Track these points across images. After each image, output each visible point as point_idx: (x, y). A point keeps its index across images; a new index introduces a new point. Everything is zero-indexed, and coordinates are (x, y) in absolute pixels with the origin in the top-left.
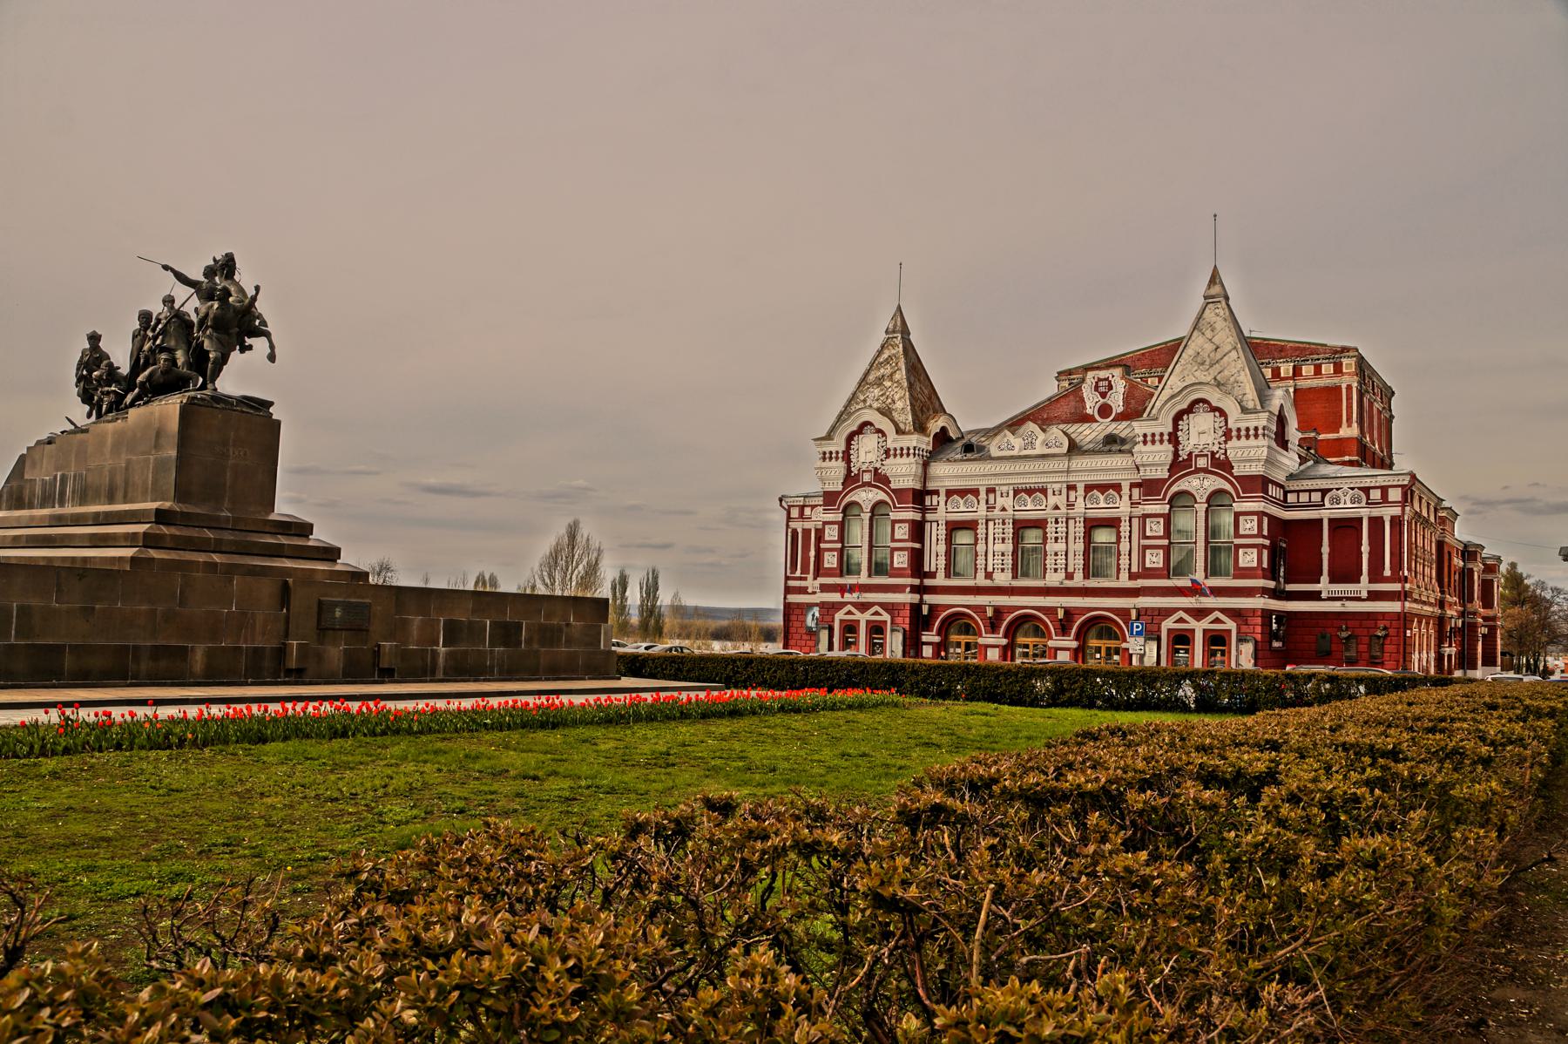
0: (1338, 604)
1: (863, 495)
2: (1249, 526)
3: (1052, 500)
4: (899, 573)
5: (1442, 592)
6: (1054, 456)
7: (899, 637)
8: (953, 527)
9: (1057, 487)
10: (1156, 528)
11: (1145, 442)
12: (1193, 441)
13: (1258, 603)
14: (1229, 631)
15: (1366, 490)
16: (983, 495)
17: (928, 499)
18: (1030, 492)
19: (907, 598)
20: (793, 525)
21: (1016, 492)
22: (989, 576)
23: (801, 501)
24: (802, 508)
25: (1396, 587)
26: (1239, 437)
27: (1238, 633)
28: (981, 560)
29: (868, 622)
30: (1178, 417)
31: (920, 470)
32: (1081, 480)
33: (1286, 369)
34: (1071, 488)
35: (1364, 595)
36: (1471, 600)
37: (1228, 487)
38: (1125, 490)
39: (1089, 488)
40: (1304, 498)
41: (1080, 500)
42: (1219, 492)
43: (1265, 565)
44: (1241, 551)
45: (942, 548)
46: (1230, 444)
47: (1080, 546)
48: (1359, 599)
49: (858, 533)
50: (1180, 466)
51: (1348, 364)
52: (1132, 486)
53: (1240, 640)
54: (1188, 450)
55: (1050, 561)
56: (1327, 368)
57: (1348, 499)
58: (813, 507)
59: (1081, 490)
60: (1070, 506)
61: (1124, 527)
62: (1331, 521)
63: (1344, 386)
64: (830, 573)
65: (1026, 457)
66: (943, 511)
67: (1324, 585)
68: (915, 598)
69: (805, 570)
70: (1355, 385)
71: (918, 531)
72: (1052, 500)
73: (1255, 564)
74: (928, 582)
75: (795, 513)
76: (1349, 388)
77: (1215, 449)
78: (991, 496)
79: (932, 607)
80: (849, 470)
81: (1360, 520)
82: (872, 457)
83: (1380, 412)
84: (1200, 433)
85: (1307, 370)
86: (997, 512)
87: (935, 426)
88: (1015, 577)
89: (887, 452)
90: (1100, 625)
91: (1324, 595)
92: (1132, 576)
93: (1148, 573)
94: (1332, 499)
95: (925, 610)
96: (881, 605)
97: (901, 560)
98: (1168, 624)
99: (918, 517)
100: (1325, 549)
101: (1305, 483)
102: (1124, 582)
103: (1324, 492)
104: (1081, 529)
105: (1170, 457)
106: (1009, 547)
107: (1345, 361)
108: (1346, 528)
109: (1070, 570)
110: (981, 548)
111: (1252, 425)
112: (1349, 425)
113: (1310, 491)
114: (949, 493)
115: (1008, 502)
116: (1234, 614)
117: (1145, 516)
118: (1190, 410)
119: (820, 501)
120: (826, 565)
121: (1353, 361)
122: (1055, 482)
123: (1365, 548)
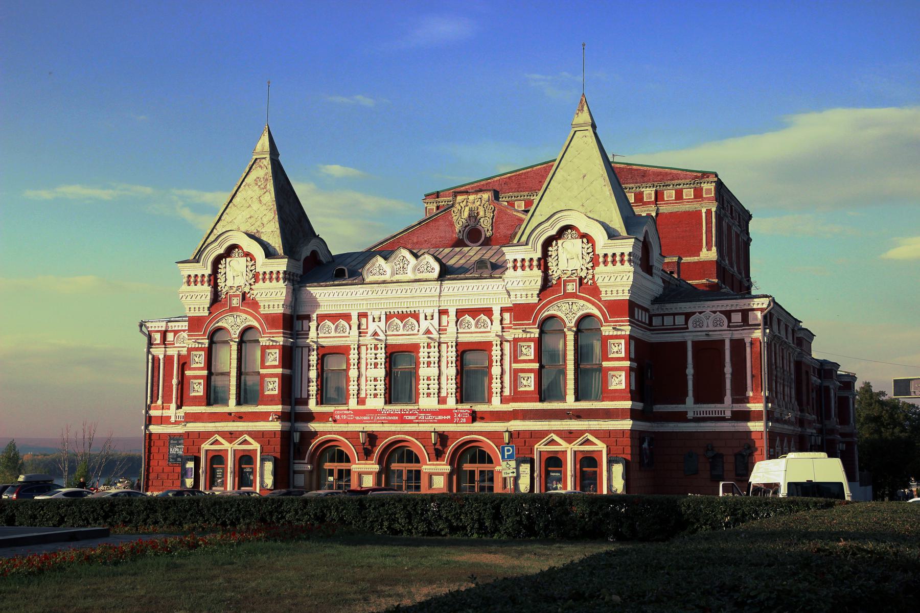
1: (231, 319)
2: (618, 349)
3: (424, 325)
4: (270, 400)
5: (801, 410)
7: (269, 466)
8: (325, 353)
10: (529, 352)
12: (563, 265)
13: (626, 424)
15: (728, 314)
17: (298, 325)
18: (402, 317)
21: (389, 317)
22: (361, 401)
23: (162, 326)
24: (164, 334)
28: (353, 388)
34: (443, 312)
35: (728, 414)
36: (828, 417)
37: (596, 312)
39: (460, 313)
40: (668, 321)
43: (633, 387)
45: (313, 374)
47: (452, 371)
48: (723, 419)
49: (228, 359)
51: (709, 187)
52: (503, 310)
53: (610, 462)
54: (556, 275)
55: (422, 386)
56: (688, 193)
57: (710, 322)
58: (176, 332)
60: (441, 330)
61: (496, 352)
62: (693, 342)
63: (704, 211)
64: (196, 401)
67: (690, 406)
70: (714, 209)
72: (424, 325)
75: (157, 337)
76: (709, 212)
77: (583, 274)
78: (364, 321)
81: (723, 342)
82: (240, 281)
83: (737, 236)
84: (569, 258)
85: (669, 194)
87: (306, 252)
88: (388, 401)
89: (256, 277)
90: (472, 452)
91: (690, 415)
93: (517, 396)
94: (695, 322)
95: (297, 437)
96: (250, 433)
97: (273, 388)
98: (540, 446)
100: (690, 371)
101: (668, 306)
102: (496, 404)
103: (688, 316)
105: (539, 283)
106: (381, 372)
107: (705, 186)
110: (353, 373)
112: (709, 249)
113: (674, 315)
116: (600, 434)
117: (516, 341)
119: (185, 325)
120: (193, 394)
121: (712, 187)
123: (728, 369)
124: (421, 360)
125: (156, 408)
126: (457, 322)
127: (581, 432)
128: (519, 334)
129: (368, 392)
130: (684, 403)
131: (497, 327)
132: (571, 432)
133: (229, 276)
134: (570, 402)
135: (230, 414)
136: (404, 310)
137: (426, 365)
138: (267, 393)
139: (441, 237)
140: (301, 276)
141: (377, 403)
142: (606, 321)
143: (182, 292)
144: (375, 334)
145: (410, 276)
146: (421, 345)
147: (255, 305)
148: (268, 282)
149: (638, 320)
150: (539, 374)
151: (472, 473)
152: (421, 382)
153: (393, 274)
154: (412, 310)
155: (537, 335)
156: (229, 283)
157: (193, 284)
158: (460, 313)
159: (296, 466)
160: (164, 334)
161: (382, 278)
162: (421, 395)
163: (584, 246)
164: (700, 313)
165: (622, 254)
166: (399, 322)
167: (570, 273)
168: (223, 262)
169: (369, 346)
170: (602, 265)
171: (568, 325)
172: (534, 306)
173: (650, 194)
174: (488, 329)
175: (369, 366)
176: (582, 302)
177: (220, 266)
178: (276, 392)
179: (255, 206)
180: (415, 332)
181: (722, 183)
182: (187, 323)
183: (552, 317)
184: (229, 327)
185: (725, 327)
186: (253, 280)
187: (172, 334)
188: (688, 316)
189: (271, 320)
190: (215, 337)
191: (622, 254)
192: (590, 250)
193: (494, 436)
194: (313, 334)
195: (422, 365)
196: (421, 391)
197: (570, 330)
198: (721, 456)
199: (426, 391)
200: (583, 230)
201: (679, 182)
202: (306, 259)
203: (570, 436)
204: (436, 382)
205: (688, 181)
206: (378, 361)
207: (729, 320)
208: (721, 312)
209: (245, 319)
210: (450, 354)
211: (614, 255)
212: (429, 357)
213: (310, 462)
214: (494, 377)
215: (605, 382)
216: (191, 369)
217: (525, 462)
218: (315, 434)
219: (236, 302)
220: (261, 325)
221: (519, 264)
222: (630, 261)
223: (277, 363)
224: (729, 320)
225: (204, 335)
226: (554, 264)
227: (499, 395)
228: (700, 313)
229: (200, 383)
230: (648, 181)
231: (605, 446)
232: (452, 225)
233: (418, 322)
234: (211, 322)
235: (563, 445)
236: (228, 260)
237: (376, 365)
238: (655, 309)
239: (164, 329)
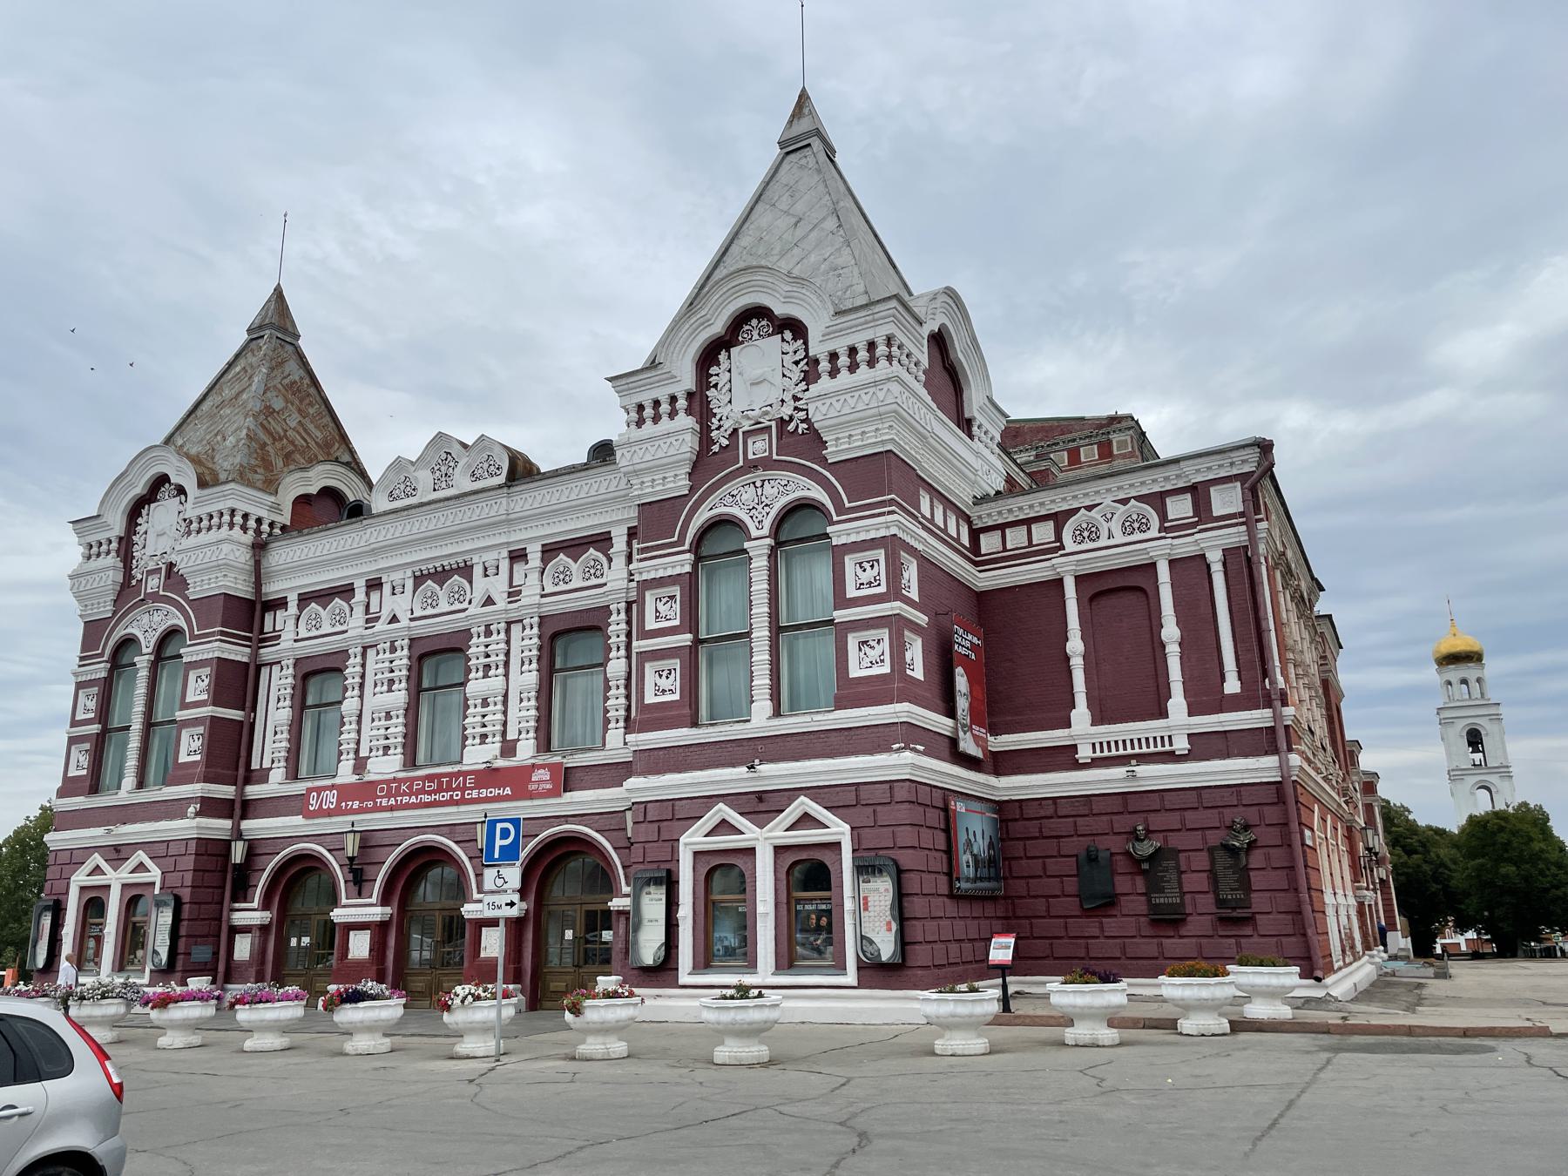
0: (1119, 772)
9: (489, 557)
14: (836, 846)
15: (1157, 500)
18: (441, 576)
21: (419, 580)
22: (360, 765)
25: (1257, 718)
30: (709, 357)
31: (243, 557)
32: (533, 538)
34: (518, 556)
35: (1181, 745)
37: (818, 494)
38: (619, 544)
39: (549, 551)
40: (1016, 538)
41: (534, 577)
42: (800, 508)
43: (918, 673)
44: (852, 641)
46: (815, 389)
48: (1171, 757)
50: (711, 461)
53: (865, 869)
57: (1115, 526)
59: (535, 559)
60: (514, 594)
62: (1079, 579)
65: (429, 503)
66: (293, 636)
68: (219, 827)
71: (237, 684)
73: (886, 669)
74: (253, 791)
77: (786, 411)
78: (375, 596)
86: (380, 626)
91: (1084, 753)
93: (641, 718)
94: (1079, 536)
95: (238, 853)
97: (190, 748)
98: (693, 839)
99: (240, 654)
100: (1075, 645)
102: (618, 744)
103: (1059, 519)
106: (399, 697)
107: (1116, 438)
108: (1119, 591)
110: (350, 705)
111: (860, 339)
113: (1028, 522)
114: (304, 600)
117: (646, 585)
122: (488, 550)
123: (1171, 632)
130: (1069, 726)
132: (760, 796)
133: (151, 537)
134: (761, 720)
137: (481, 674)
140: (284, 528)
141: (386, 766)
142: (841, 509)
144: (394, 619)
149: (924, 517)
150: (690, 657)
155: (688, 568)
156: (149, 551)
158: (549, 551)
159: (236, 915)
163: (790, 349)
164: (1089, 508)
168: (144, 512)
170: (825, 378)
177: (140, 520)
178: (198, 758)
180: (465, 605)
181: (1143, 434)
185: (1154, 533)
188: (1059, 519)
191: (872, 346)
194: (287, 636)
200: (779, 310)
201: (1070, 436)
202: (303, 501)
203: (761, 806)
205: (1087, 432)
207: (1163, 516)
208: (1139, 498)
210: (526, 642)
213: (266, 906)
217: (657, 882)
219: (153, 584)
222: (889, 358)
224: (1163, 516)
228: (1089, 508)
233: (471, 583)
235: (751, 834)
238: (987, 515)
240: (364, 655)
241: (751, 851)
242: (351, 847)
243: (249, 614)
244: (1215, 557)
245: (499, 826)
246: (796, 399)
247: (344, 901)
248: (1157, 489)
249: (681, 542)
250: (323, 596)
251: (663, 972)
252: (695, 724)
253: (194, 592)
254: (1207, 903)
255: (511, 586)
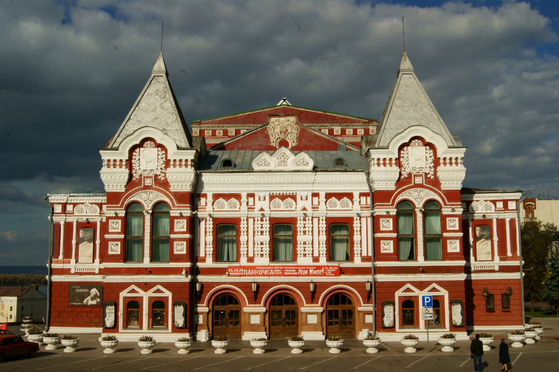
4: (179, 258)
6: (304, 171)
9: (304, 194)
11: (379, 165)
15: (494, 202)
16: (244, 198)
18: (283, 197)
19: (184, 278)
20: (56, 219)
21: (272, 197)
22: (251, 260)
24: (64, 205)
26: (445, 164)
27: (450, 297)
28: (243, 249)
29: (150, 298)
33: (337, 130)
34: (315, 195)
35: (497, 268)
39: (328, 196)
42: (430, 202)
45: (210, 238)
46: (439, 168)
47: (323, 238)
48: (493, 271)
49: (144, 227)
54: (408, 171)
55: (300, 248)
58: (75, 205)
60: (315, 208)
61: (356, 224)
64: (114, 258)
66: (208, 209)
69: (68, 255)
72: (301, 204)
74: (200, 265)
75: (58, 209)
77: (427, 171)
78: (251, 200)
79: (202, 285)
80: (131, 176)
81: (491, 221)
85: (349, 131)
89: (167, 163)
92: (364, 259)
96: (163, 284)
97: (181, 248)
98: (399, 293)
102: (358, 262)
104: (323, 225)
106: (266, 238)
109: (316, 254)
110: (243, 238)
111: (454, 157)
114: (216, 196)
115: (265, 204)
118: (407, 145)
120: (110, 253)
122: (303, 191)
124: (298, 229)
125: (58, 262)
126: (326, 202)
127: (430, 283)
128: (380, 211)
129: (256, 252)
131: (357, 207)
132: (421, 282)
134: (421, 261)
135: (146, 269)
136: (285, 193)
138: (175, 252)
139: (259, 145)
142: (445, 204)
143: (103, 173)
144: (262, 210)
145: (290, 166)
146: (299, 218)
147: (165, 184)
148: (178, 167)
151: (337, 312)
152: (299, 245)
153: (276, 166)
154: (291, 193)
156: (142, 168)
157: (112, 167)
160: (64, 205)
161: (267, 168)
162: (299, 255)
163: (427, 151)
165: (457, 159)
166: (280, 201)
167: (418, 170)
169: (256, 219)
170: (442, 165)
171: (417, 206)
172: (392, 192)
173: (338, 131)
174: (350, 208)
175: (256, 233)
176: (427, 191)
177: (134, 154)
179: (159, 111)
180: (293, 208)
182: (106, 198)
183: (405, 202)
184: (142, 201)
185: (493, 210)
186: (164, 165)
187: (72, 206)
189: (180, 197)
190: (133, 209)
191: (457, 159)
192: (432, 154)
193: (359, 286)
194: (209, 208)
195: (299, 233)
196: (299, 252)
197: (148, 213)
198: (492, 295)
199: (303, 252)
200: (428, 140)
204: (311, 245)
206: (264, 229)
208: (490, 201)
209: (155, 196)
211: (451, 159)
212: (304, 227)
214: (355, 242)
215: (445, 247)
216: (109, 233)
218: (212, 285)
220: (171, 200)
221: (381, 162)
223: (185, 230)
225: (121, 206)
226: (406, 163)
227: (359, 255)
229: (117, 245)
230: (337, 123)
231: (447, 292)
232: (267, 137)
234: (127, 197)
236: (142, 149)
237: (262, 233)
239: (65, 202)
240: (247, 220)
241: (417, 297)
242: (254, 287)
243: (193, 198)
244: (508, 220)
245: (426, 298)
246: (430, 167)
247: (248, 305)
248: (495, 199)
249: (393, 204)
250: (227, 197)
251: (391, 329)
252: (398, 260)
253: (172, 189)
254: (500, 308)
255: (312, 204)
